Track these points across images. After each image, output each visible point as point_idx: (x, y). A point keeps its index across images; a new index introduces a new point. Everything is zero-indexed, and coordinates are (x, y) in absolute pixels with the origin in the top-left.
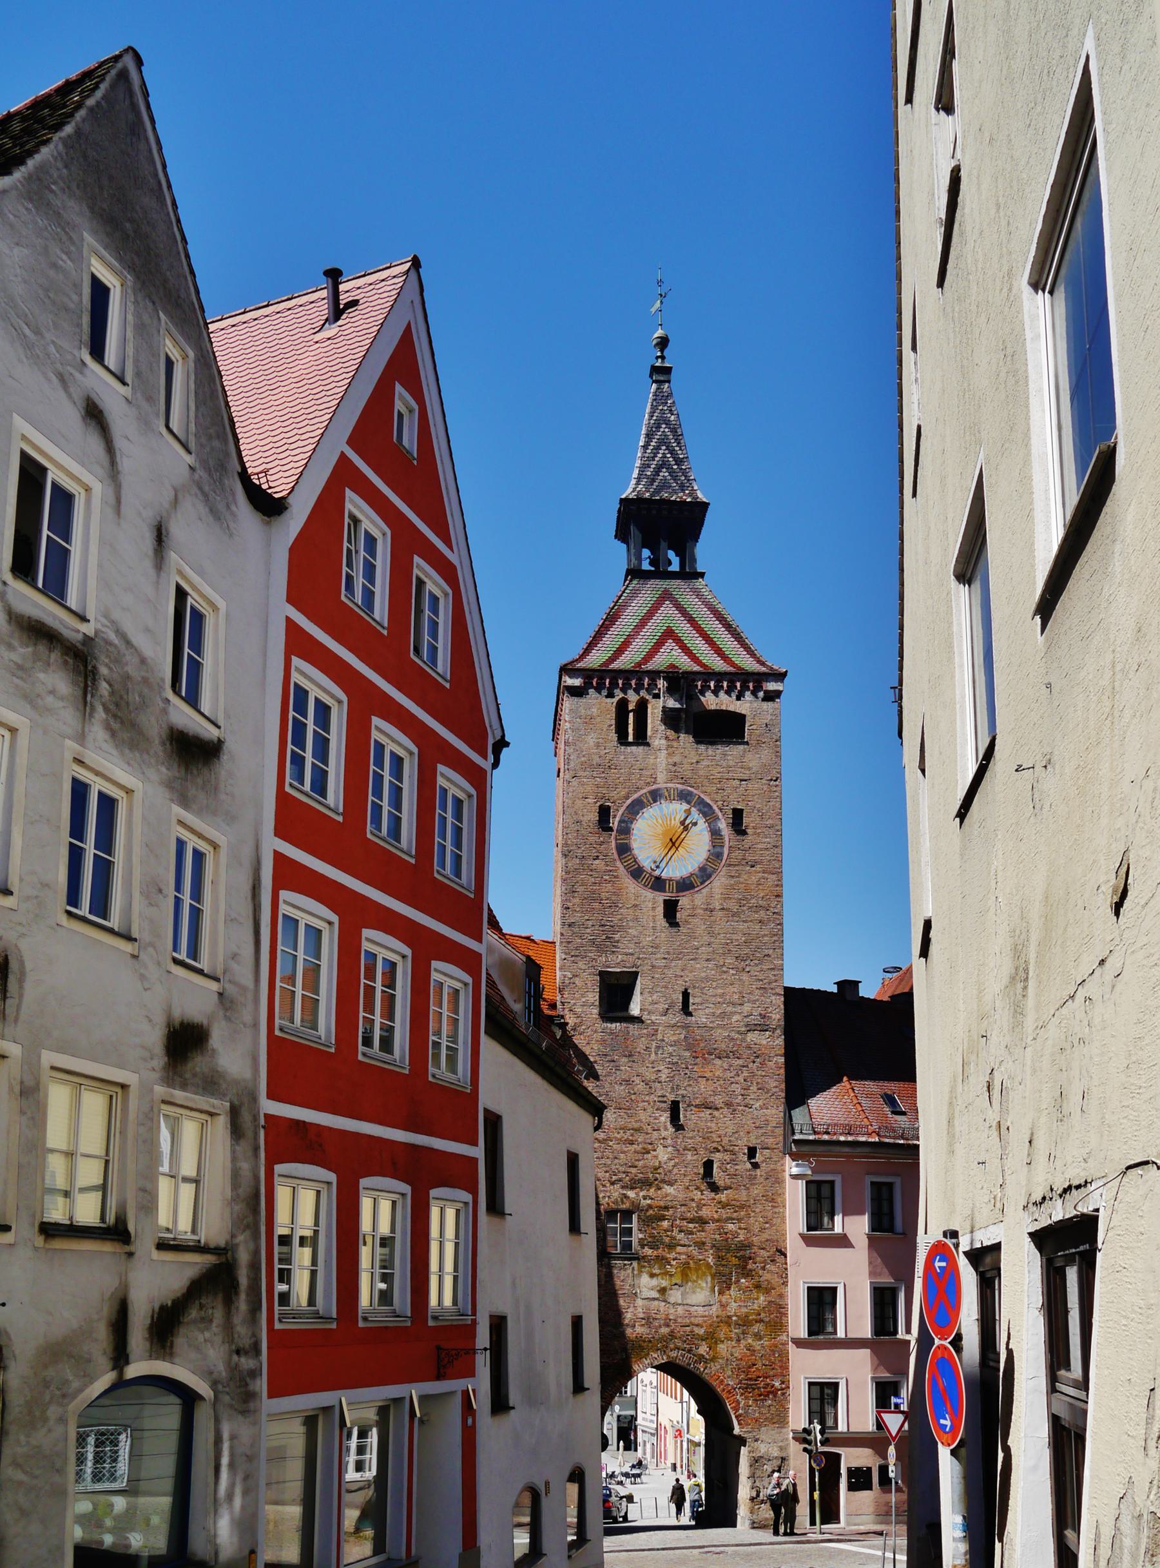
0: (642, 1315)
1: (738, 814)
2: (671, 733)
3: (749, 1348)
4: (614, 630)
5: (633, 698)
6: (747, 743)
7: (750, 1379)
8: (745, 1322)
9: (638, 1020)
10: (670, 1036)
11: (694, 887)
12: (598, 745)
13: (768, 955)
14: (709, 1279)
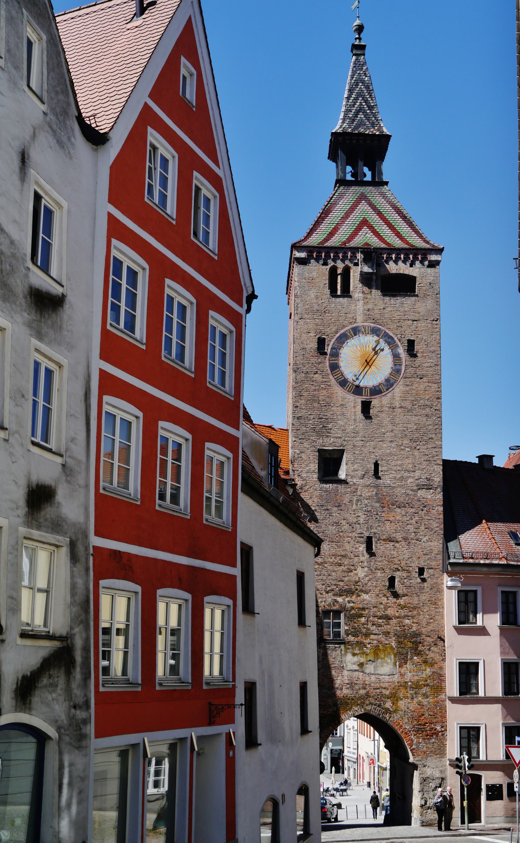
0: (347, 682)
1: (411, 344)
2: (366, 289)
3: (420, 703)
4: (327, 220)
5: (340, 266)
6: (417, 296)
7: (420, 725)
8: (417, 686)
9: (344, 482)
10: (366, 493)
11: (382, 392)
12: (317, 297)
13: (432, 438)
14: (393, 657)
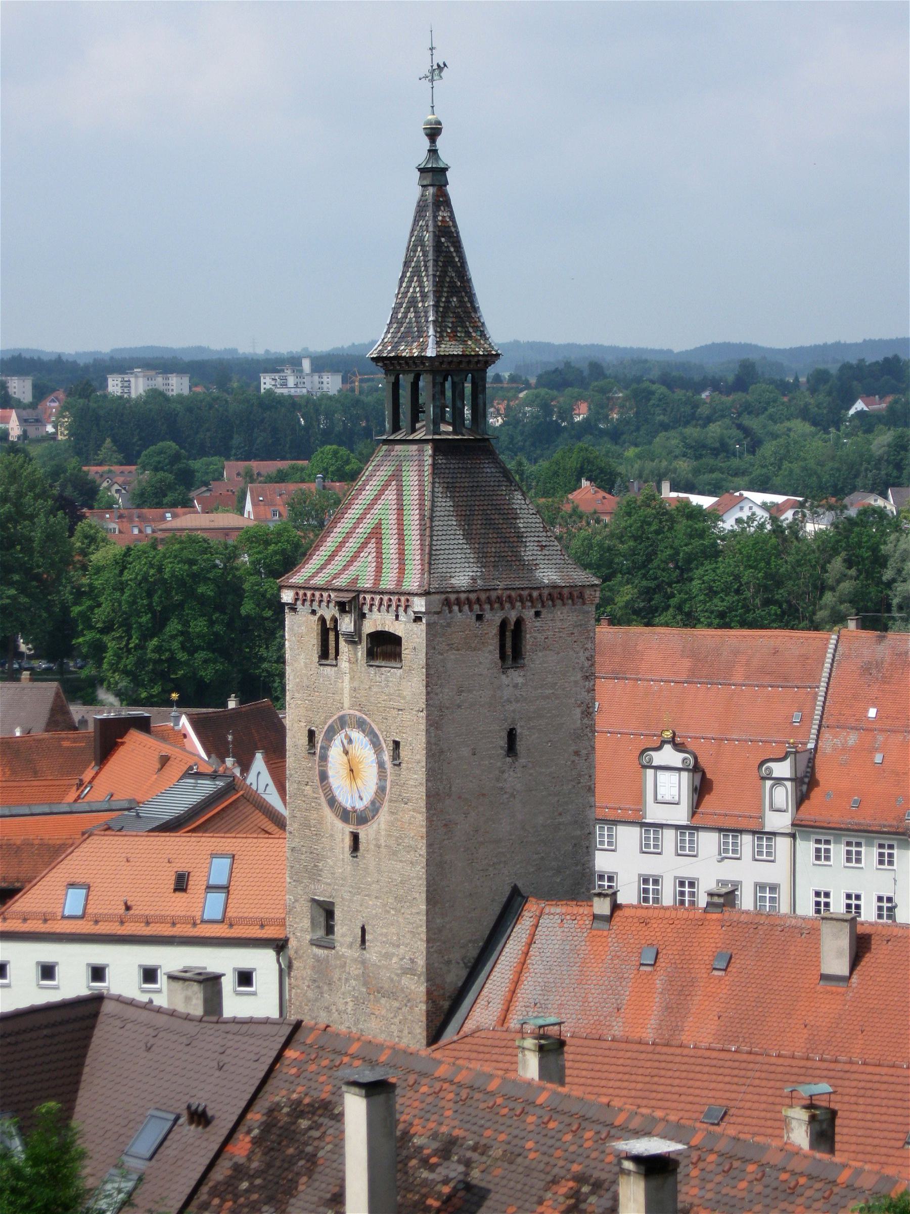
1: (397, 744)
